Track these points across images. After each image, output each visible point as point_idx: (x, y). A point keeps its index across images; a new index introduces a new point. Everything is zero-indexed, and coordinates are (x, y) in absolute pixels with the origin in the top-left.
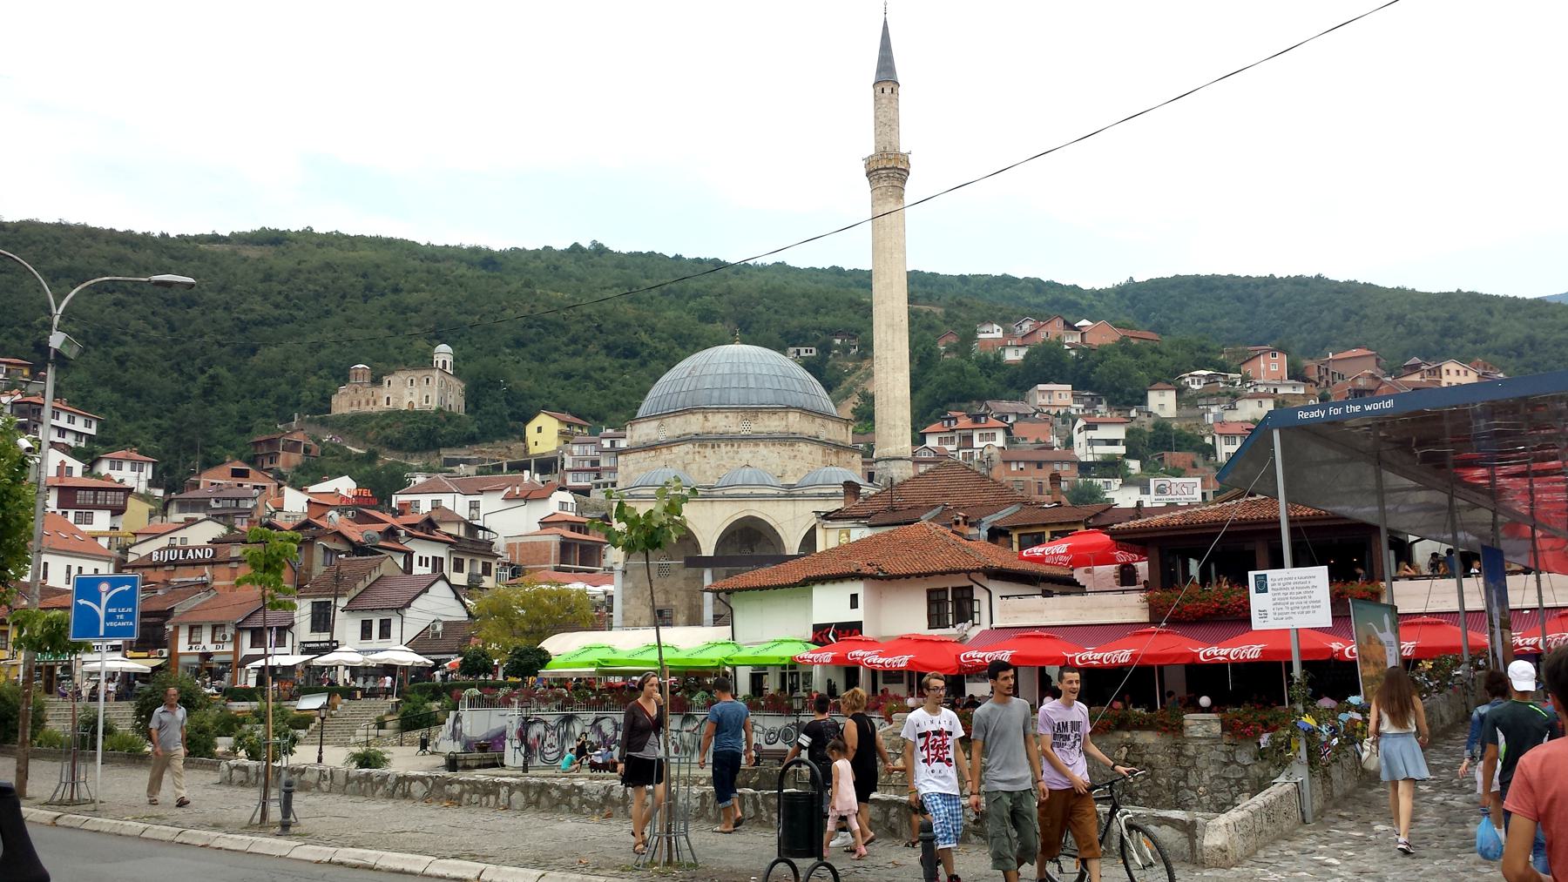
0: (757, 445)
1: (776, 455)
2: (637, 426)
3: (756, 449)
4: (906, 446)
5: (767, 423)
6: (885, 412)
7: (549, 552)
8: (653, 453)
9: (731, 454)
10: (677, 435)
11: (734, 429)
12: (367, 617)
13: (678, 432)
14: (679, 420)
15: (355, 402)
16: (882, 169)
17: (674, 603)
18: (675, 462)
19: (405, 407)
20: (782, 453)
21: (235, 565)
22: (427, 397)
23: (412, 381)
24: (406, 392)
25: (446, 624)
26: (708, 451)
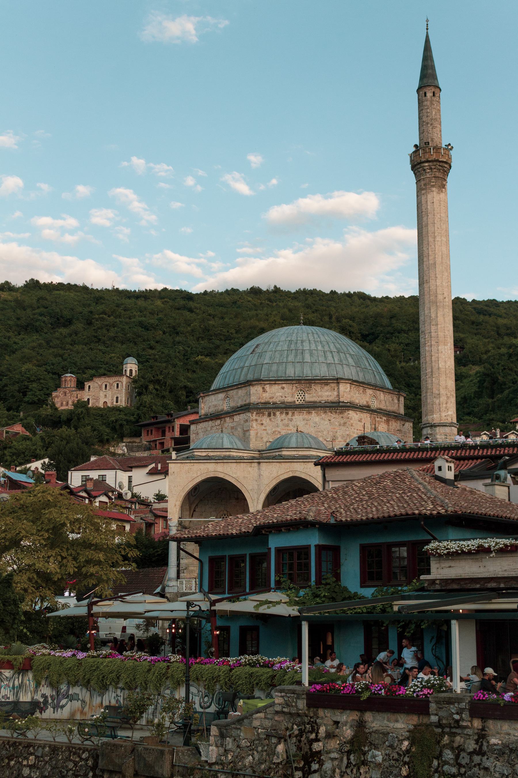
0: (309, 413)
1: (327, 422)
4: (450, 413)
5: (320, 393)
6: (430, 381)
8: (218, 422)
9: (286, 422)
10: (239, 405)
11: (289, 399)
14: (241, 392)
15: (64, 403)
18: (236, 429)
19: (101, 405)
20: (333, 420)
22: (117, 398)
23: (106, 386)
24: (102, 394)
26: (265, 420)
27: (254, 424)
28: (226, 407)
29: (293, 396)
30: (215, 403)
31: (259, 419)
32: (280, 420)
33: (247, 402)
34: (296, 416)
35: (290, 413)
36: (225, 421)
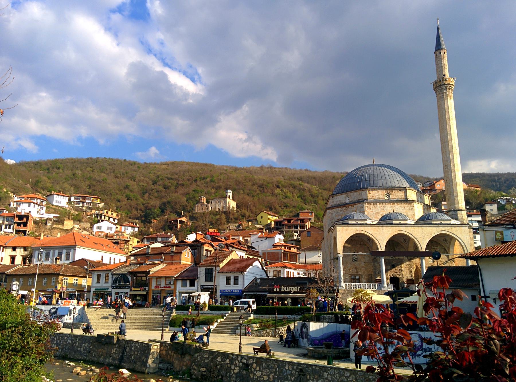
0: (394, 204)
1: (403, 208)
2: (335, 197)
3: (394, 206)
5: (397, 194)
8: (345, 208)
9: (382, 208)
10: (355, 200)
11: (382, 197)
16: (443, 85)
17: (360, 273)
21: (173, 254)
25: (261, 279)
26: (372, 207)
27: (366, 209)
29: (384, 195)
30: (340, 199)
31: (369, 206)
32: (379, 207)
33: (360, 198)
34: (387, 205)
35: (384, 203)
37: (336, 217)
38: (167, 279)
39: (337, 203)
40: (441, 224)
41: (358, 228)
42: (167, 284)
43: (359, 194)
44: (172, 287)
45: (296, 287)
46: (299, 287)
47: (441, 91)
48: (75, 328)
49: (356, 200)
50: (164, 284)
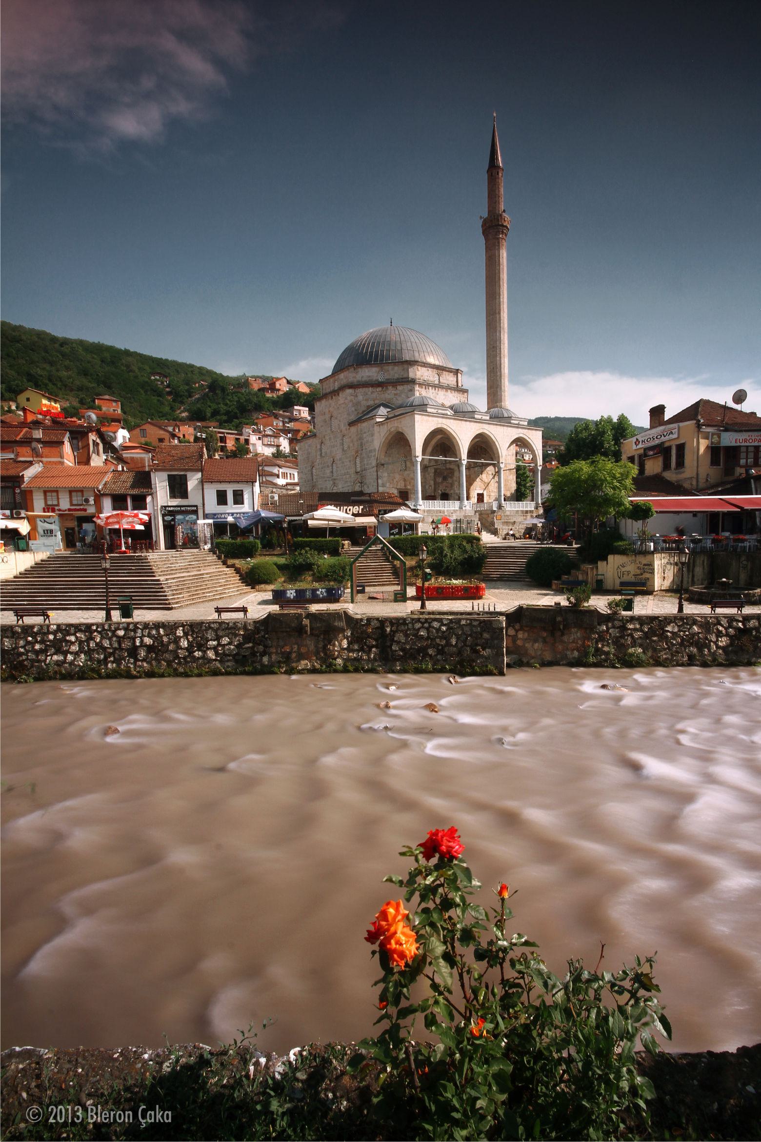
0: (447, 391)
2: (360, 370)
3: (447, 394)
7: (145, 463)
8: (380, 389)
10: (395, 378)
11: (431, 379)
12: (222, 487)
13: (396, 376)
17: (409, 487)
28: (381, 378)
30: (368, 374)
31: (420, 389)
36: (387, 389)
37: (365, 402)
38: (48, 494)
39: (363, 380)
40: (518, 424)
41: (440, 420)
42: (75, 502)
43: (404, 369)
44: (91, 510)
45: (357, 507)
46: (361, 507)
47: (496, 235)
48: (429, 599)
49: (398, 379)
50: (69, 504)
